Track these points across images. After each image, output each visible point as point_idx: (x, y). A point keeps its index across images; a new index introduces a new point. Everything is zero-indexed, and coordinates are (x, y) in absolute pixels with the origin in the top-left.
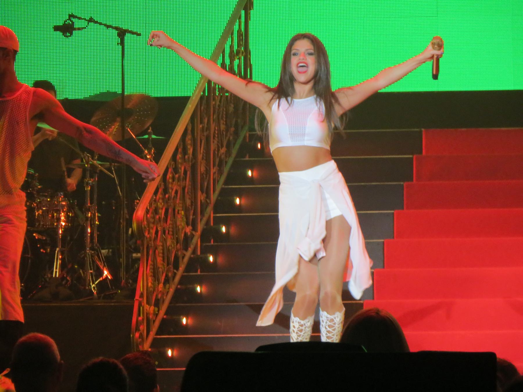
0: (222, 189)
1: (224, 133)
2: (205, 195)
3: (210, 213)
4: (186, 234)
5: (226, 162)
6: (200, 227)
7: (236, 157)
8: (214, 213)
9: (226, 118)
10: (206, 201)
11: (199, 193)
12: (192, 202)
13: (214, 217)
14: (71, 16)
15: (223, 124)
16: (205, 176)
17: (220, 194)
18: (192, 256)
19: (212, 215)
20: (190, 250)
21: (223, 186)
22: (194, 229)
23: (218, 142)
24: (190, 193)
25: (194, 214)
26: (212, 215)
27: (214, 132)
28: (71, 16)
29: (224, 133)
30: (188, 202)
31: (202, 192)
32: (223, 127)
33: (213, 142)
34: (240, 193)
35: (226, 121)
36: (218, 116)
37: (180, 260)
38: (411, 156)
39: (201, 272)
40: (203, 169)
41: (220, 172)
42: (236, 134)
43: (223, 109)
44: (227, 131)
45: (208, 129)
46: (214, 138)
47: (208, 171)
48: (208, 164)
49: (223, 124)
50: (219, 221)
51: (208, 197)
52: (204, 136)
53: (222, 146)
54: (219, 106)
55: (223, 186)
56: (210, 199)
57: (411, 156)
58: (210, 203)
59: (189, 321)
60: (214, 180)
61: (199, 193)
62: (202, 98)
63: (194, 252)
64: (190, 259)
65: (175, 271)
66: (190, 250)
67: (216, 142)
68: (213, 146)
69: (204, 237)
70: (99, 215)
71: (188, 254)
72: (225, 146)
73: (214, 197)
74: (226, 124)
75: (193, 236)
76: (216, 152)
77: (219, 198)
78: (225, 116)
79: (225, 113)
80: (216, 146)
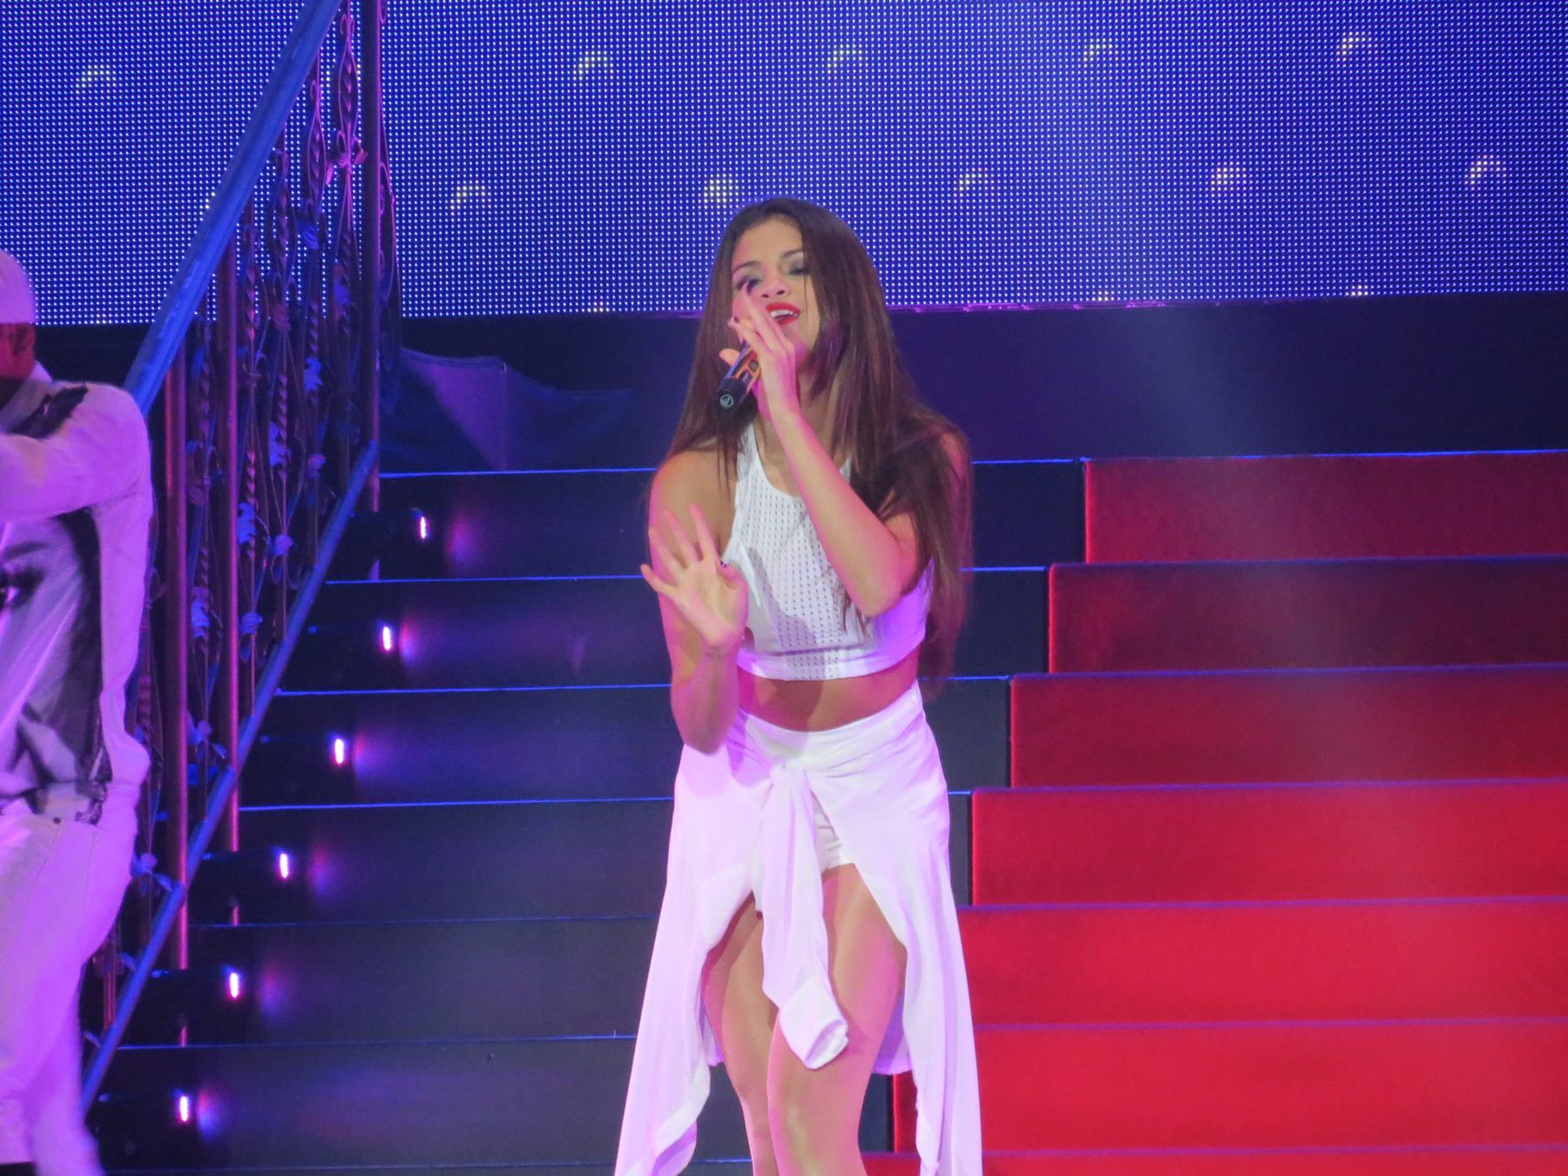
0: (276, 703)
1: (284, 478)
2: (204, 729)
3: (230, 797)
5: (292, 595)
7: (335, 569)
8: (242, 803)
9: (291, 415)
10: (212, 751)
11: (185, 717)
13: (241, 815)
15: (279, 439)
16: (206, 651)
17: (266, 727)
18: (156, 974)
19: (235, 811)
21: (279, 692)
23: (259, 513)
24: (147, 723)
26: (235, 811)
27: (244, 477)
29: (284, 478)
31: (197, 720)
33: (240, 513)
35: (290, 429)
36: (260, 408)
37: (110, 988)
38: (1041, 569)
40: (199, 620)
41: (269, 637)
42: (332, 478)
43: (279, 383)
45: (220, 458)
46: (242, 499)
47: (217, 634)
49: (279, 439)
51: (219, 735)
52: (202, 487)
53: (275, 532)
55: (279, 692)
56: (227, 746)
57: (1041, 569)
58: (228, 760)
60: (243, 668)
61: (185, 717)
62: (193, 331)
63: (165, 958)
65: (89, 1036)
67: (249, 515)
68: (240, 530)
69: (204, 897)
71: (143, 967)
72: (285, 529)
73: (241, 743)
74: (291, 442)
75: (159, 897)
76: (252, 555)
77: (265, 739)
78: (284, 409)
79: (284, 394)
80: (252, 529)
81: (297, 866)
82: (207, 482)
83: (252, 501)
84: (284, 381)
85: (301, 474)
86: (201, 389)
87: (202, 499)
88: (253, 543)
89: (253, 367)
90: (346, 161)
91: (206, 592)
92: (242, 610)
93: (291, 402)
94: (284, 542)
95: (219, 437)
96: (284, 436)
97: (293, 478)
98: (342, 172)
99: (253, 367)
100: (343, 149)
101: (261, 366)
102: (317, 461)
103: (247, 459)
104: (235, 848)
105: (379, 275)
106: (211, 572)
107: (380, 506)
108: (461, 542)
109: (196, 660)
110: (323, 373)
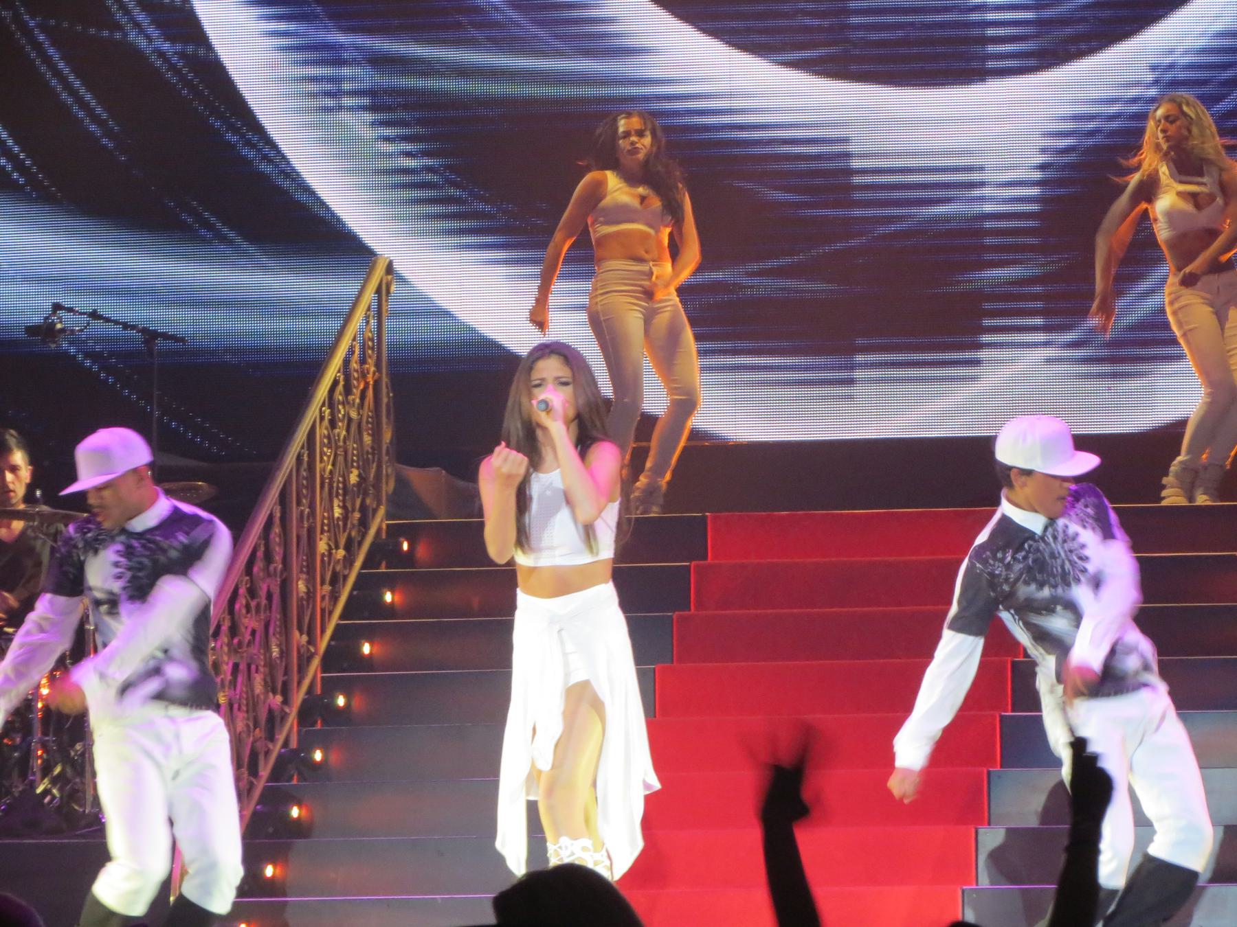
4: (270, 711)
6: (299, 697)
9: (345, 495)
12: (282, 652)
14: (57, 307)
19: (319, 675)
20: (281, 738)
22: (286, 702)
25: (287, 672)
28: (57, 307)
30: (275, 652)
31: (301, 634)
32: (337, 512)
34: (369, 633)
37: (261, 757)
39: (299, 780)
41: (334, 598)
44: (345, 518)
45: (313, 513)
47: (310, 594)
48: (311, 581)
50: (331, 687)
54: (331, 472)
59: (278, 871)
60: (323, 610)
61: (297, 633)
64: (280, 756)
66: (281, 738)
68: (322, 546)
70: (384, 564)
71: (277, 749)
74: (344, 507)
75: (284, 716)
92: (323, 583)
106: (308, 566)
110: (359, 476)
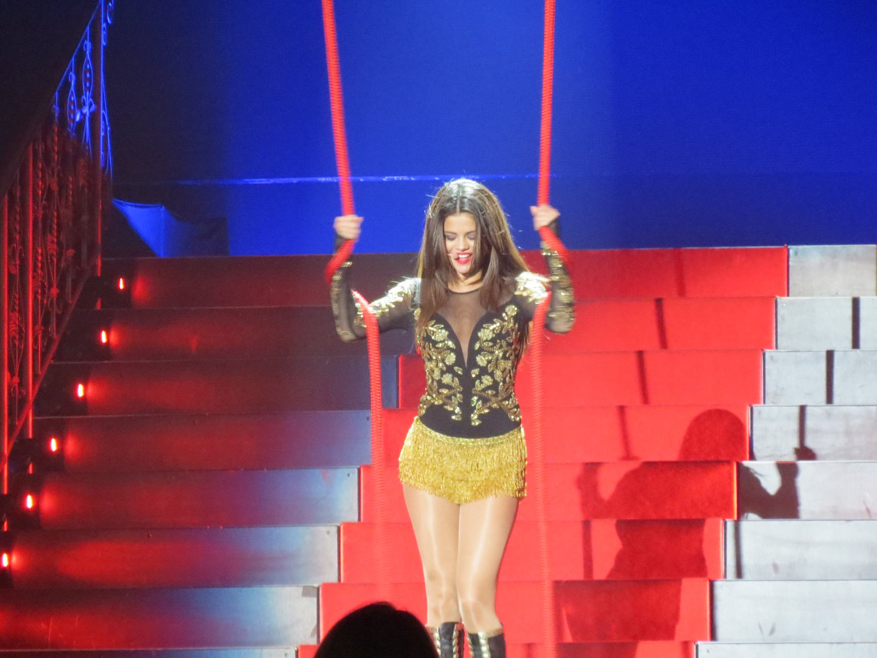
1: (55, 260)
16: (17, 343)
32: (53, 249)
33: (34, 277)
44: (60, 255)
46: (35, 271)
74: (59, 243)
81: (61, 444)
82: (18, 262)
83: (40, 272)
84: (55, 214)
85: (63, 259)
86: (15, 219)
87: (16, 271)
88: (40, 291)
89: (40, 208)
90: (86, 110)
91: (17, 314)
92: (34, 324)
93: (58, 225)
94: (55, 291)
95: (23, 242)
96: (55, 240)
97: (59, 260)
98: (83, 115)
99: (40, 208)
100: (84, 104)
101: (44, 208)
102: (71, 252)
103: (37, 252)
104: (31, 436)
105: (101, 164)
107: (102, 273)
108: (140, 290)
109: (12, 347)
